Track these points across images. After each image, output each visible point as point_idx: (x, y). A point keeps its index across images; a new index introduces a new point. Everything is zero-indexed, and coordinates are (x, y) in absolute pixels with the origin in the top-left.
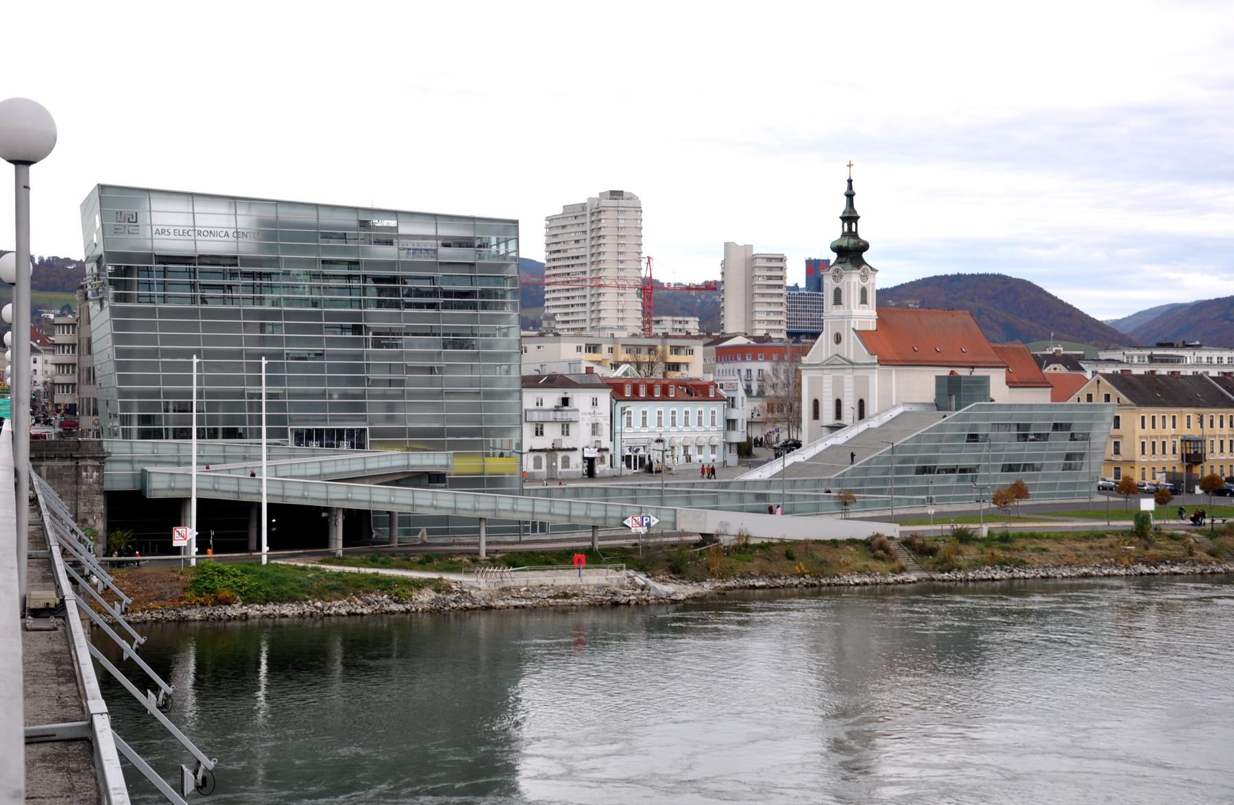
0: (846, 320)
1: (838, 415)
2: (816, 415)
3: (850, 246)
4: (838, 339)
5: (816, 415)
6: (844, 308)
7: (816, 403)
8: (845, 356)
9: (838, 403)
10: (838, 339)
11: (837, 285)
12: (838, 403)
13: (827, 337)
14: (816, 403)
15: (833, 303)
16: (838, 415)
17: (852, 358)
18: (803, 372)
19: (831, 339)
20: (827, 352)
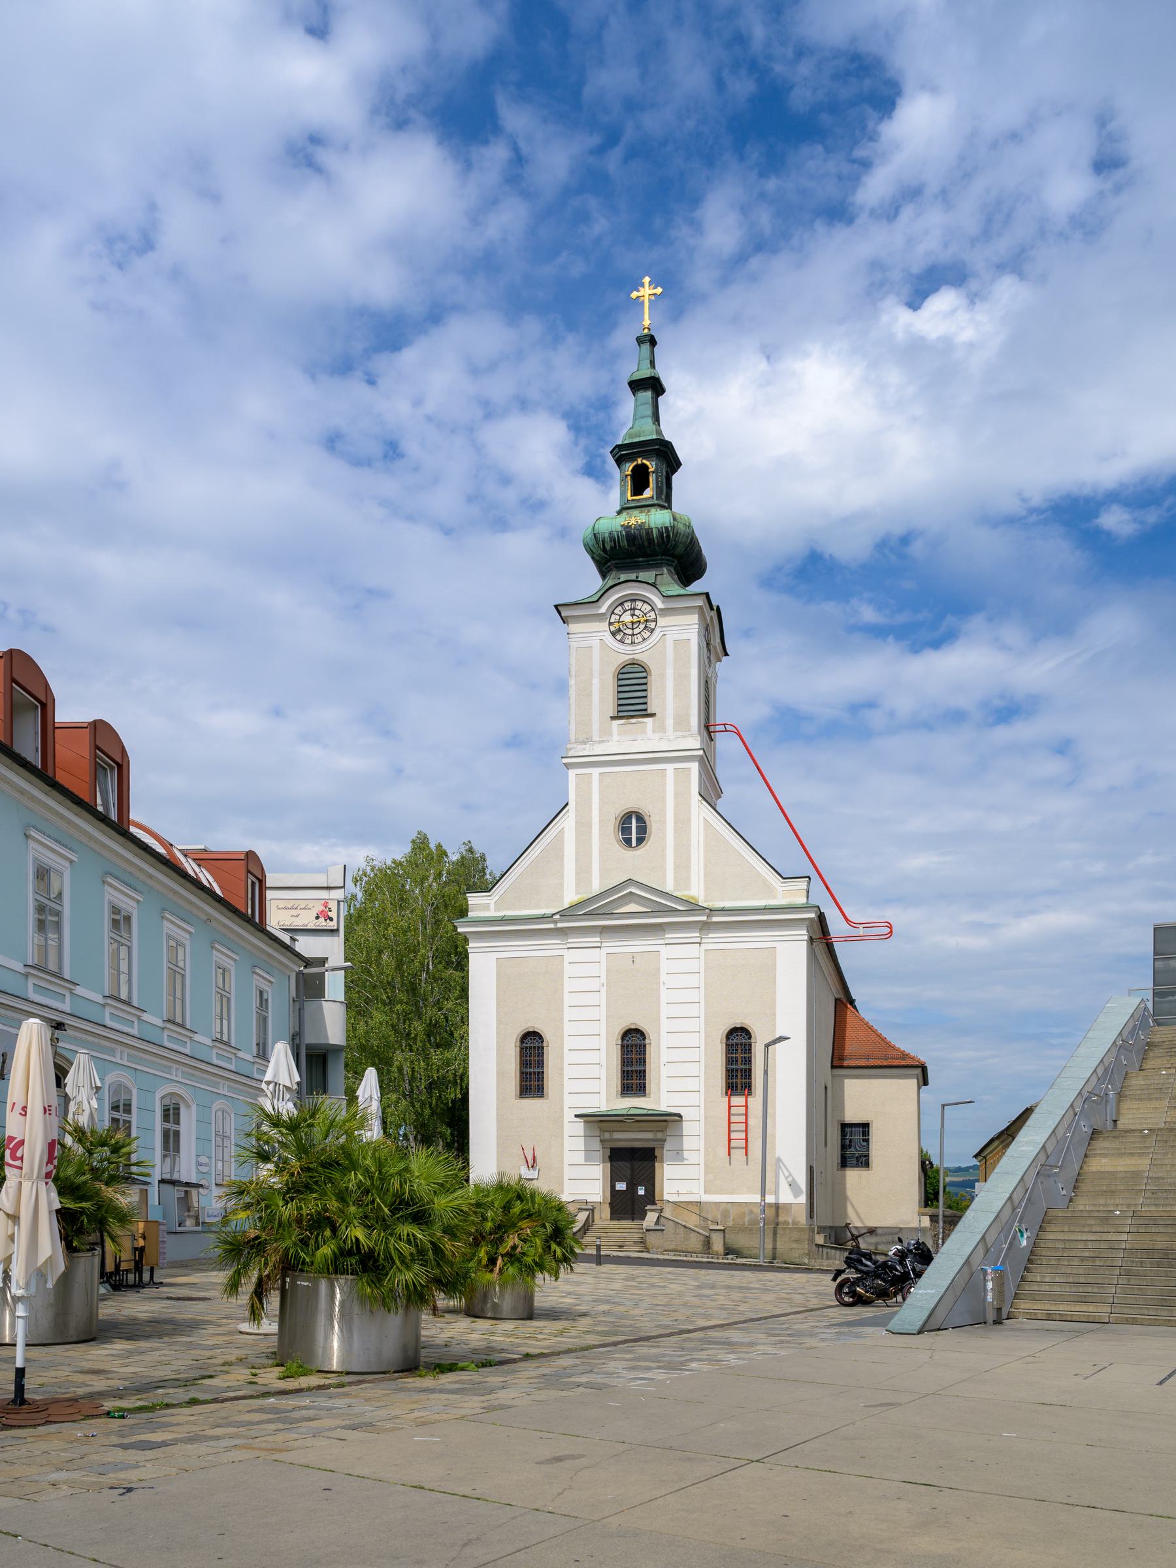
0: (670, 768)
6: (661, 728)
11: (623, 653)
13: (583, 826)
15: (611, 709)
17: (697, 891)
18: (472, 945)
20: (583, 872)
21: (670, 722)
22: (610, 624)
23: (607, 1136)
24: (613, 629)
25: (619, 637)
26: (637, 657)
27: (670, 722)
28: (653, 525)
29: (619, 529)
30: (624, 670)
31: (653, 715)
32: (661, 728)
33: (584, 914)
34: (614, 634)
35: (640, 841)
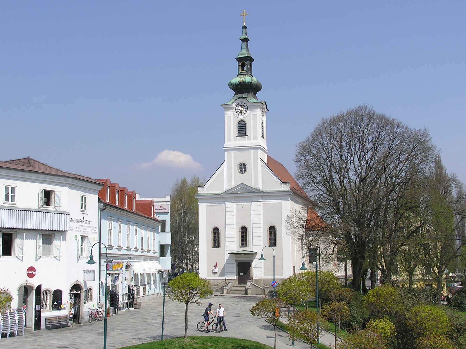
1: (244, 241)
2: (216, 242)
3: (254, 82)
4: (243, 168)
5: (216, 242)
7: (216, 231)
8: (252, 184)
9: (244, 231)
10: (243, 168)
12: (244, 231)
13: (230, 167)
14: (216, 231)
15: (236, 134)
16: (244, 241)
17: (260, 186)
19: (235, 169)
21: (252, 138)
22: (236, 109)
23: (237, 259)
24: (236, 111)
25: (238, 113)
26: (243, 119)
27: (252, 138)
28: (246, 82)
29: (238, 82)
30: (240, 122)
31: (247, 135)
32: (250, 139)
33: (230, 193)
34: (236, 112)
35: (245, 171)
